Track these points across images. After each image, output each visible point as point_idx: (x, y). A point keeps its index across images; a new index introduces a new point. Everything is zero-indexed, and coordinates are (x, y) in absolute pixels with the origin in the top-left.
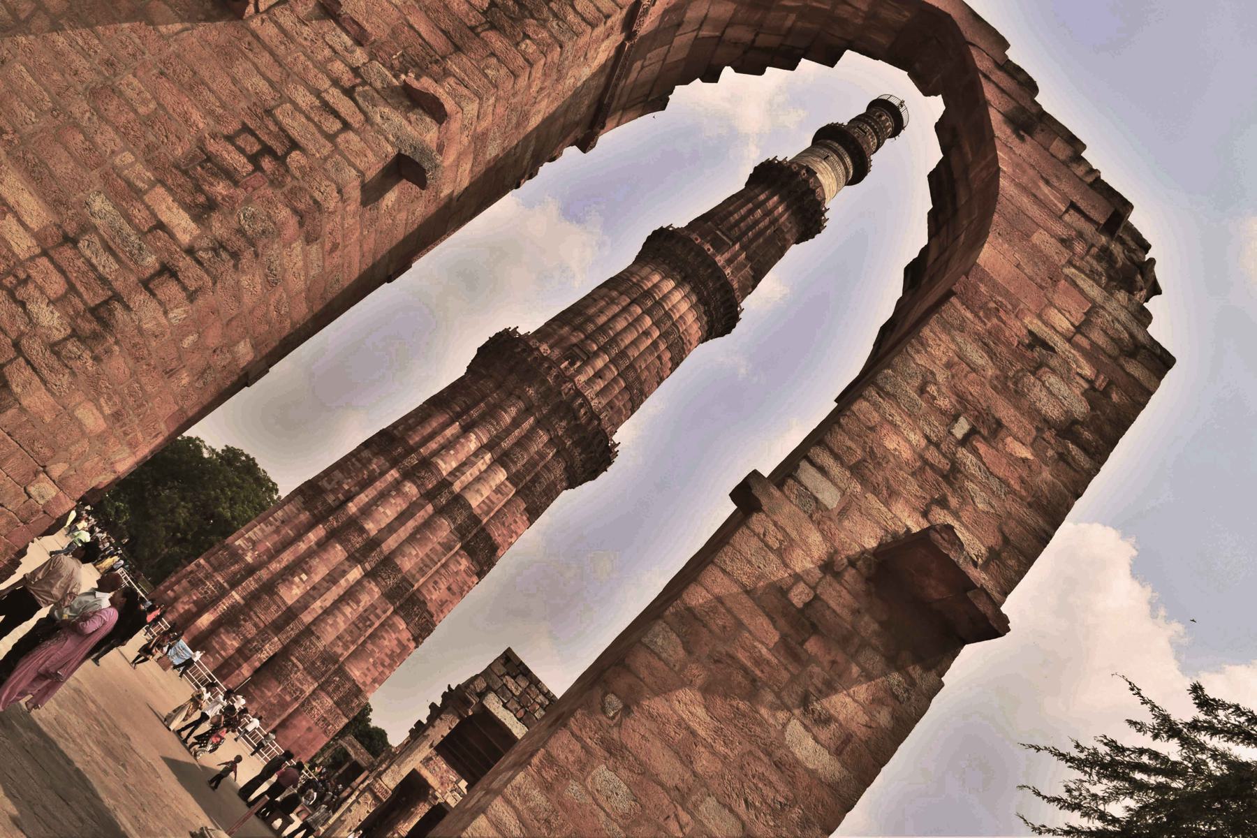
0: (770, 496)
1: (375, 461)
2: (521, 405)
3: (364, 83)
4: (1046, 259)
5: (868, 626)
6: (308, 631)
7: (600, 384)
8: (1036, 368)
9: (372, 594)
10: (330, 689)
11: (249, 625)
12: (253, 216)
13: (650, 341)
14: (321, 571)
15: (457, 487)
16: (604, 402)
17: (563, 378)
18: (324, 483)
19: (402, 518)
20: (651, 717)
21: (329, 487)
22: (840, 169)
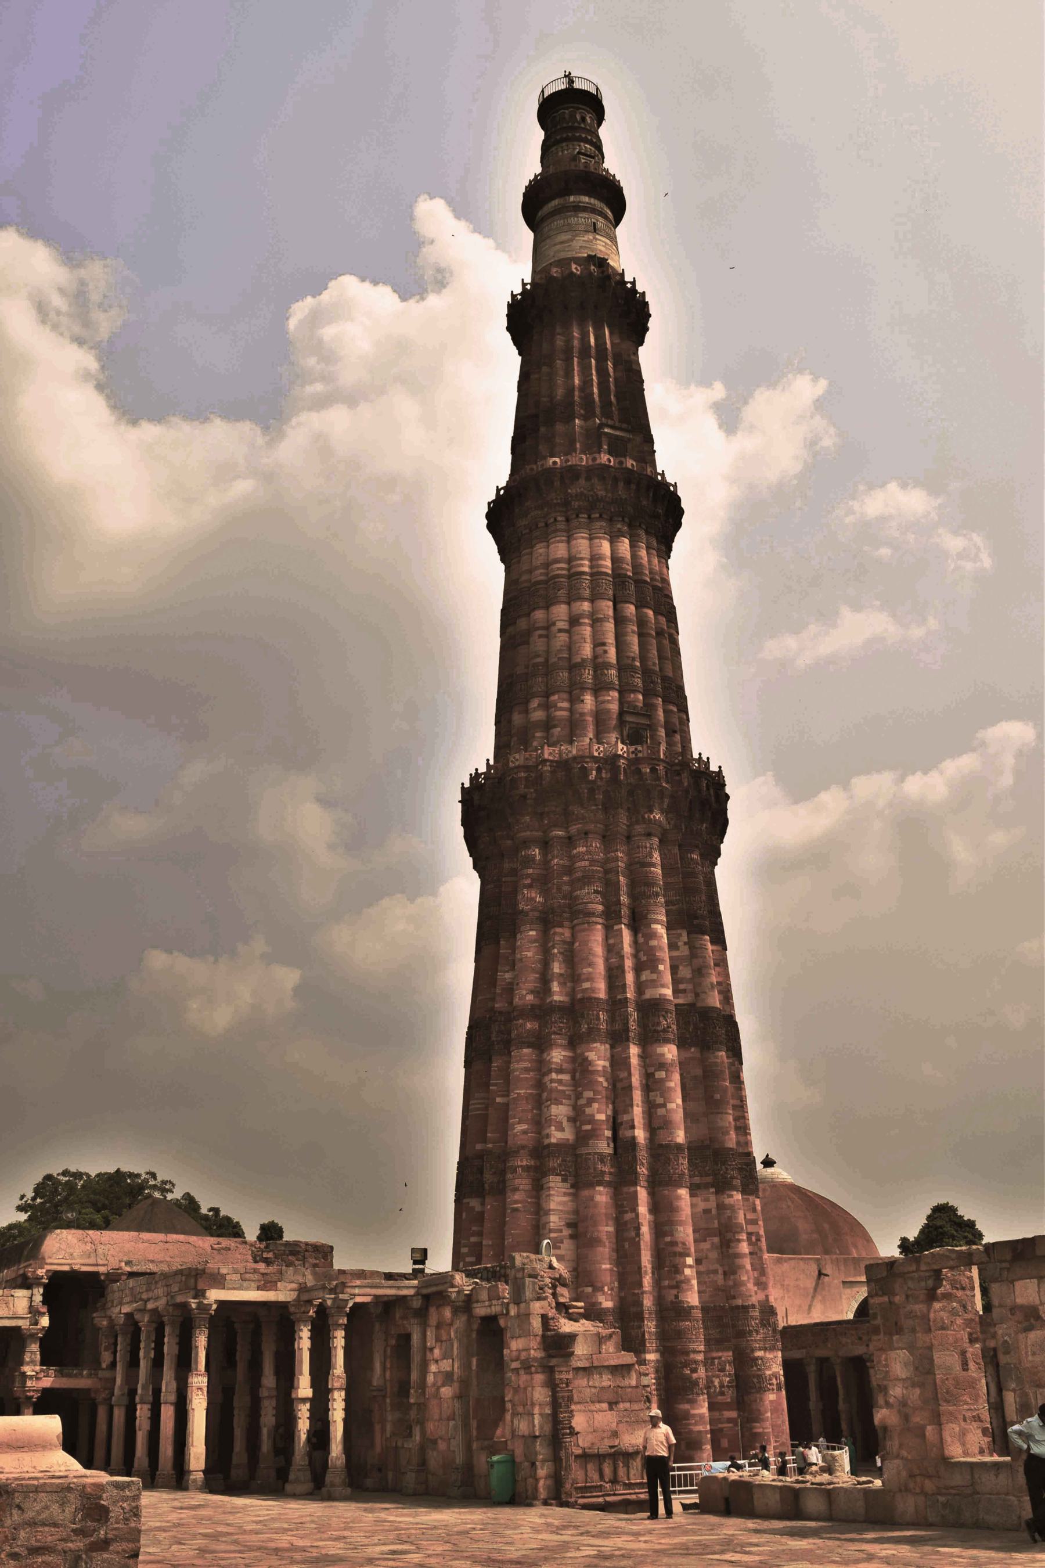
1: (592, 1056)
7: (678, 737)
14: (686, 1233)
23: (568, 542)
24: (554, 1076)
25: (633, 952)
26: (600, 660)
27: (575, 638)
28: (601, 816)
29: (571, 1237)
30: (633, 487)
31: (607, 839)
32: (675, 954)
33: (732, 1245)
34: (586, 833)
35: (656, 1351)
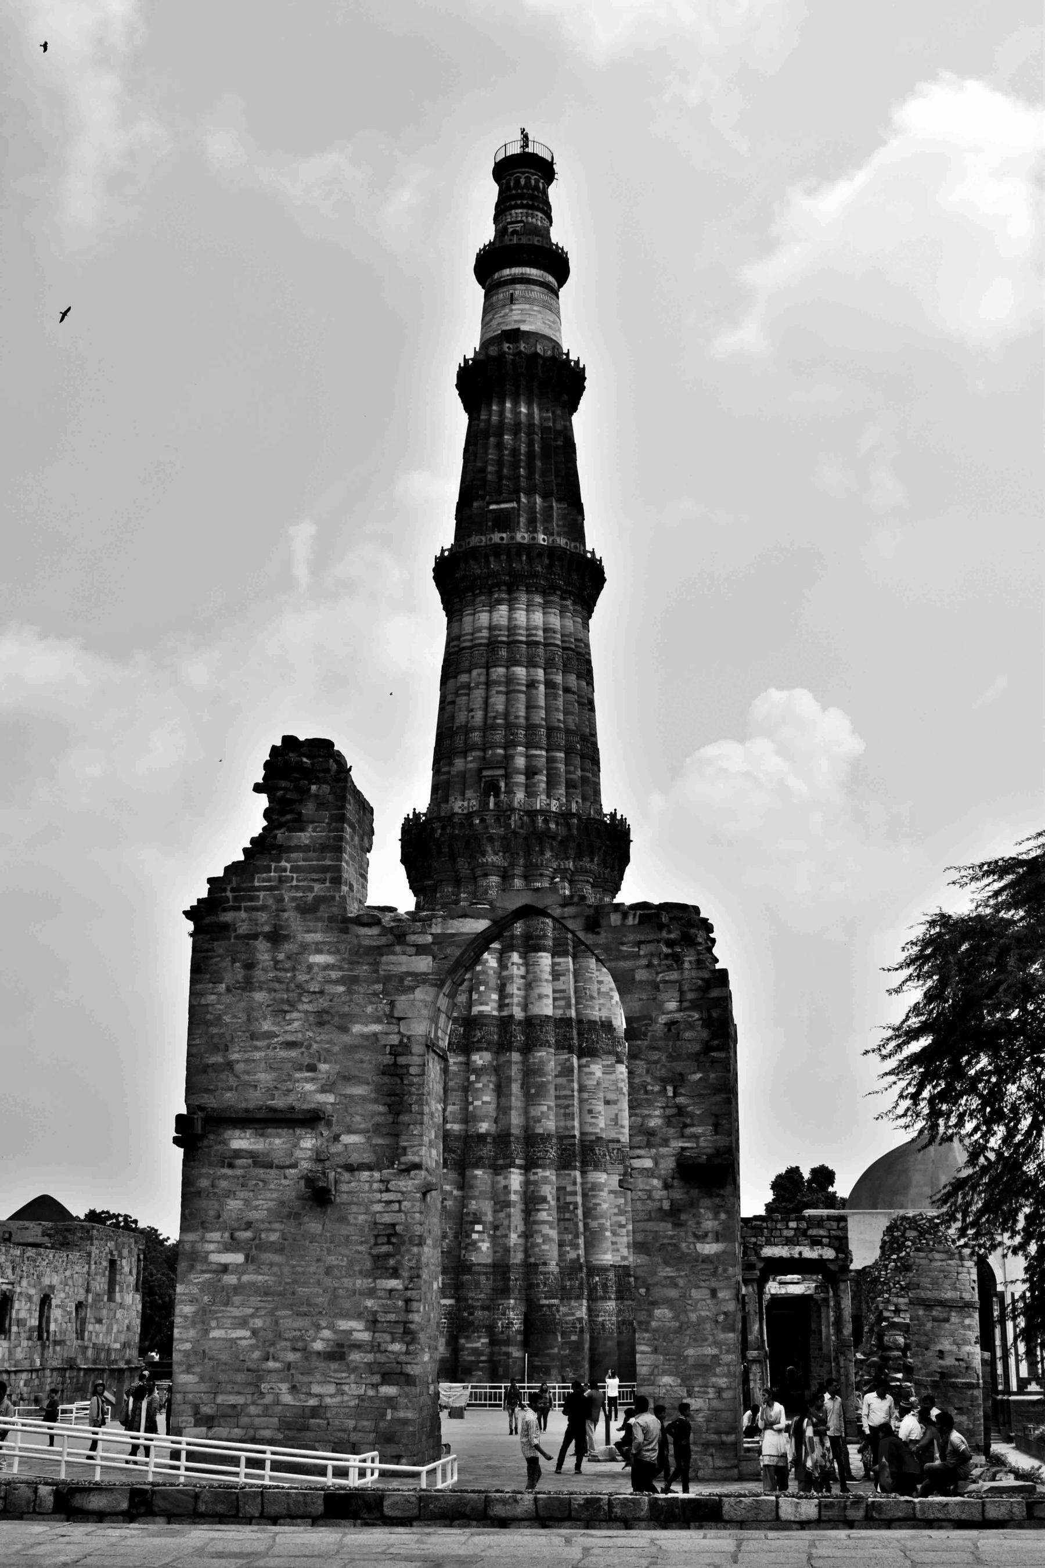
0: (631, 1183)
2: (494, 880)
3: (388, 1182)
4: (648, 982)
5: (695, 1192)
6: (531, 1268)
8: (678, 1037)
10: (600, 1293)
11: (479, 1314)
12: (409, 1260)
13: (542, 688)
16: (562, 791)
17: (504, 813)
19: (501, 1090)
20: (656, 1284)
22: (537, 292)
30: (504, 557)
31: (458, 882)
34: (441, 881)
35: (449, 1298)
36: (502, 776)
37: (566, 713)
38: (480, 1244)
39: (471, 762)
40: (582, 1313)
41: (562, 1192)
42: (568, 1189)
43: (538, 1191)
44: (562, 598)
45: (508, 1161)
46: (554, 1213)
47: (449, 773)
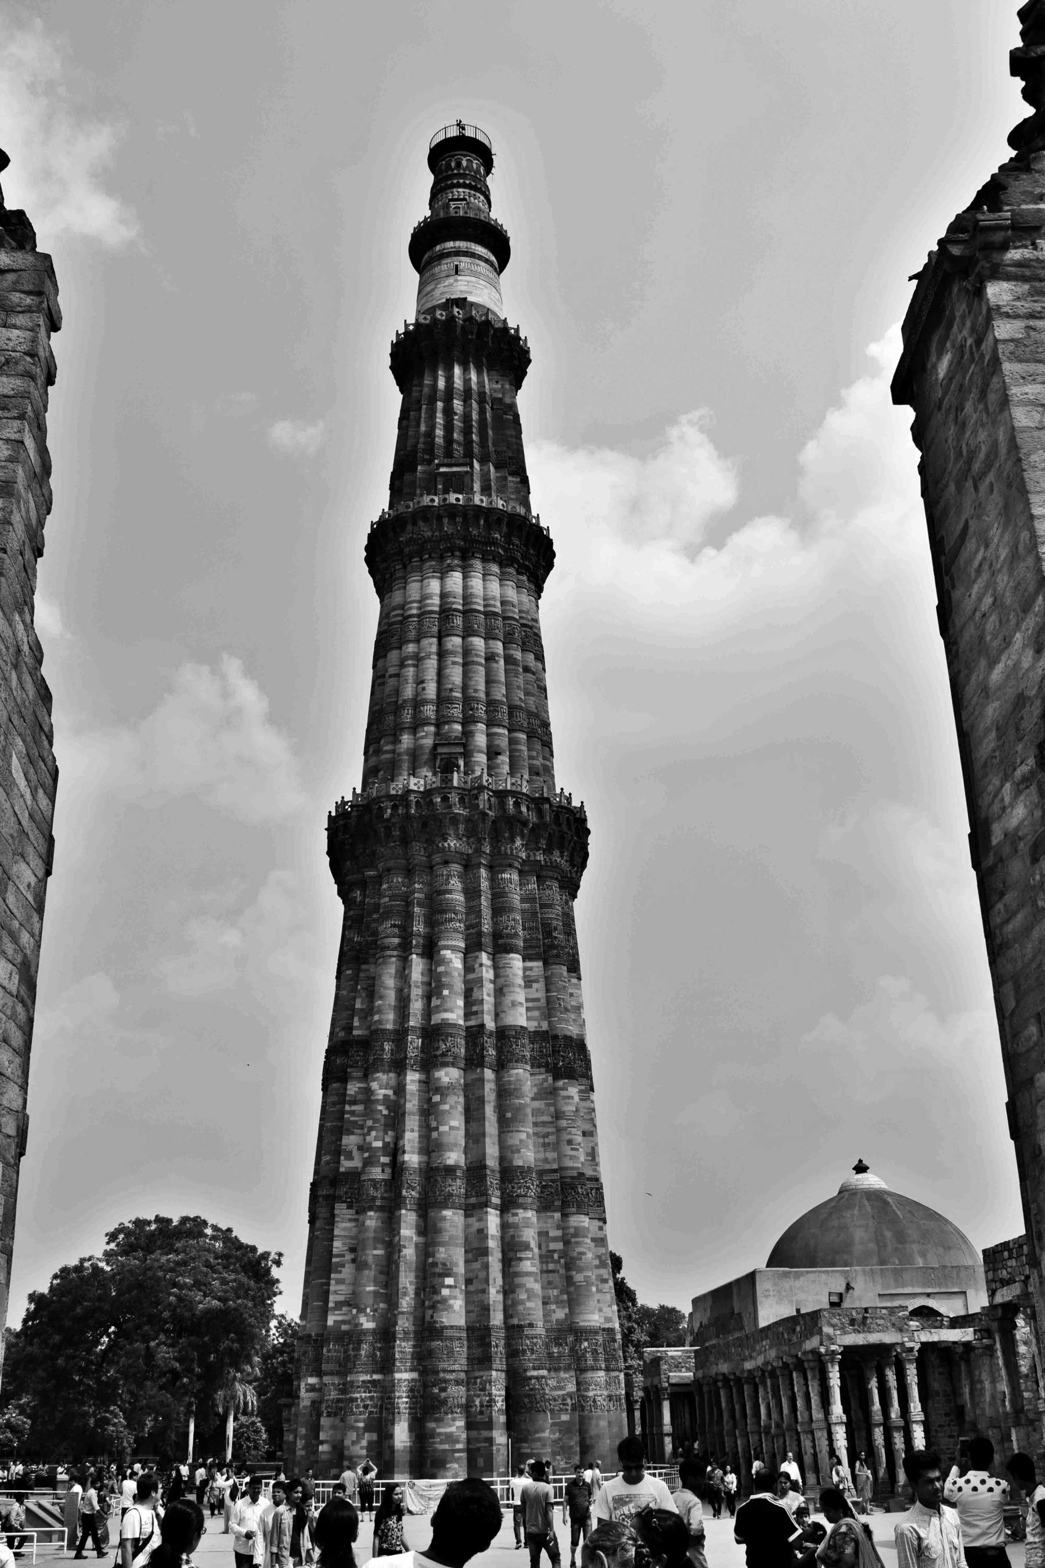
1: (374, 1085)
6: (514, 1331)
7: (504, 759)
9: (530, 1222)
10: (590, 1362)
13: (502, 662)
14: (453, 1254)
15: (490, 1024)
16: (526, 777)
18: (346, 1165)
19: (473, 1113)
21: (356, 1163)
23: (405, 588)
24: (347, 1108)
25: (426, 979)
26: (419, 698)
27: (402, 679)
28: (399, 851)
29: (354, 1261)
30: (459, 519)
31: (409, 872)
32: (471, 976)
33: (513, 1263)
34: (389, 870)
35: (411, 1370)
36: (460, 753)
37: (527, 694)
38: (451, 1302)
39: (422, 737)
40: (571, 1388)
41: (543, 1239)
42: (551, 1234)
43: (519, 1236)
44: (519, 573)
45: (483, 1199)
46: (537, 1262)
47: (393, 752)
